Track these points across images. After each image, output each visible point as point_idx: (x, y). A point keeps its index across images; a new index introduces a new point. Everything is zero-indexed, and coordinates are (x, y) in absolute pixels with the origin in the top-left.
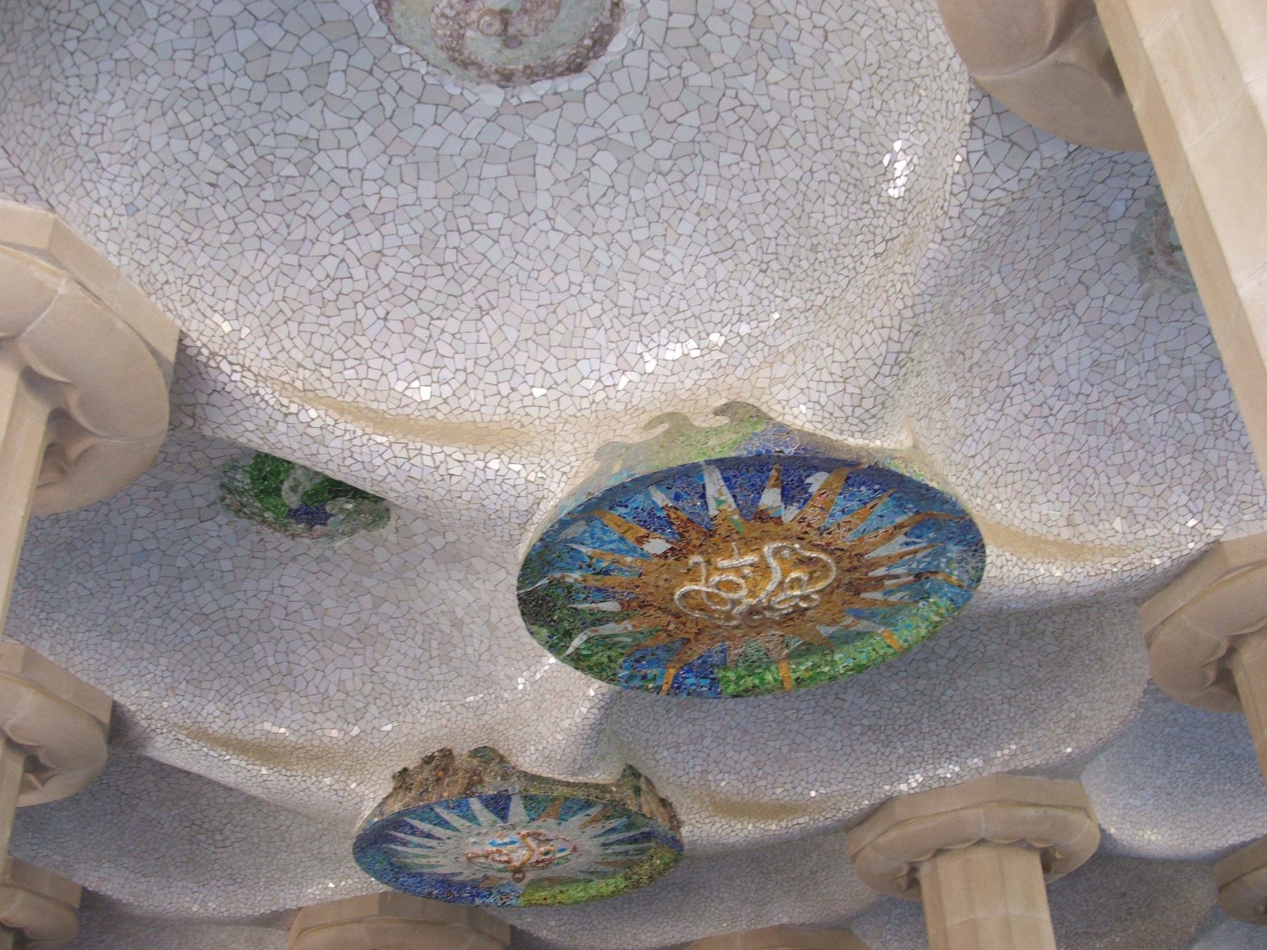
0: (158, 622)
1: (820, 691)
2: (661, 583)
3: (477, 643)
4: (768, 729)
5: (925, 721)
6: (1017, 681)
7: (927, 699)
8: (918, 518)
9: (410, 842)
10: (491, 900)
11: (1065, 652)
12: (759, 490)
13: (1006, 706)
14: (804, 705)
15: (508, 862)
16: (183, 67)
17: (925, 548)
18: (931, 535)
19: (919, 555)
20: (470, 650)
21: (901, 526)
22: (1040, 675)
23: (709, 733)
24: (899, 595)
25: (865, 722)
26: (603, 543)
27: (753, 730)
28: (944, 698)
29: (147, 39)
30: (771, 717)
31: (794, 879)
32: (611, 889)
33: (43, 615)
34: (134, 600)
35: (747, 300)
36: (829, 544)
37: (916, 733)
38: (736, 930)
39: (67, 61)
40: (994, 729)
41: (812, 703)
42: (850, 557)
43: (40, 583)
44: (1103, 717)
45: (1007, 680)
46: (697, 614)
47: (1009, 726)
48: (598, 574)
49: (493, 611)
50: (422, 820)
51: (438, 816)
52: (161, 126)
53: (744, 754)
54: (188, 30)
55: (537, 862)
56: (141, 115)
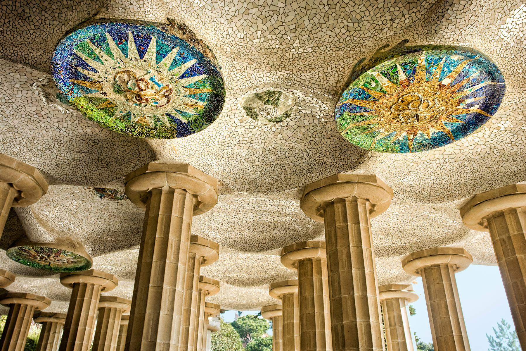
2: (421, 88)
3: (233, 9)
5: (215, 149)
6: (249, 160)
7: (223, 144)
9: (127, 45)
10: (65, 89)
11: (274, 163)
13: (237, 163)
15: (142, 90)
20: (227, 8)
22: (257, 163)
25: (204, 136)
26: (448, 67)
28: (227, 148)
31: (61, 156)
32: (113, 125)
35: (492, 50)
37: (209, 151)
38: (16, 158)
40: (227, 166)
44: (265, 186)
45: (247, 157)
46: (400, 101)
47: (232, 169)
48: (426, 69)
49: (256, 9)
50: (157, 46)
51: (168, 52)
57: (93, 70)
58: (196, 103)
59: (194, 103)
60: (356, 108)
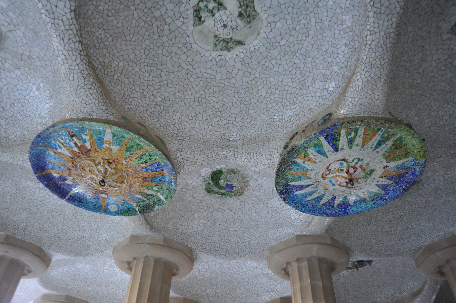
0: (281, 215)
1: (304, 12)
4: (327, 38)
8: (49, 149)
10: (418, 170)
12: (69, 185)
14: (313, 20)
16: (97, 220)
17: (59, 141)
18: (53, 142)
19: (62, 141)
21: (55, 152)
23: (323, 71)
24: (84, 137)
27: (327, 47)
29: (93, 225)
30: (320, 37)
33: (267, 239)
34: (272, 218)
36: (73, 167)
39: (96, 237)
41: (312, 15)
42: (74, 160)
43: (257, 236)
51: (315, 199)
52: (107, 224)
53: (340, 51)
54: (91, 219)
55: (347, 172)
56: (105, 227)
57: (378, 186)
58: (304, 163)
59: (306, 162)
60: (156, 169)
